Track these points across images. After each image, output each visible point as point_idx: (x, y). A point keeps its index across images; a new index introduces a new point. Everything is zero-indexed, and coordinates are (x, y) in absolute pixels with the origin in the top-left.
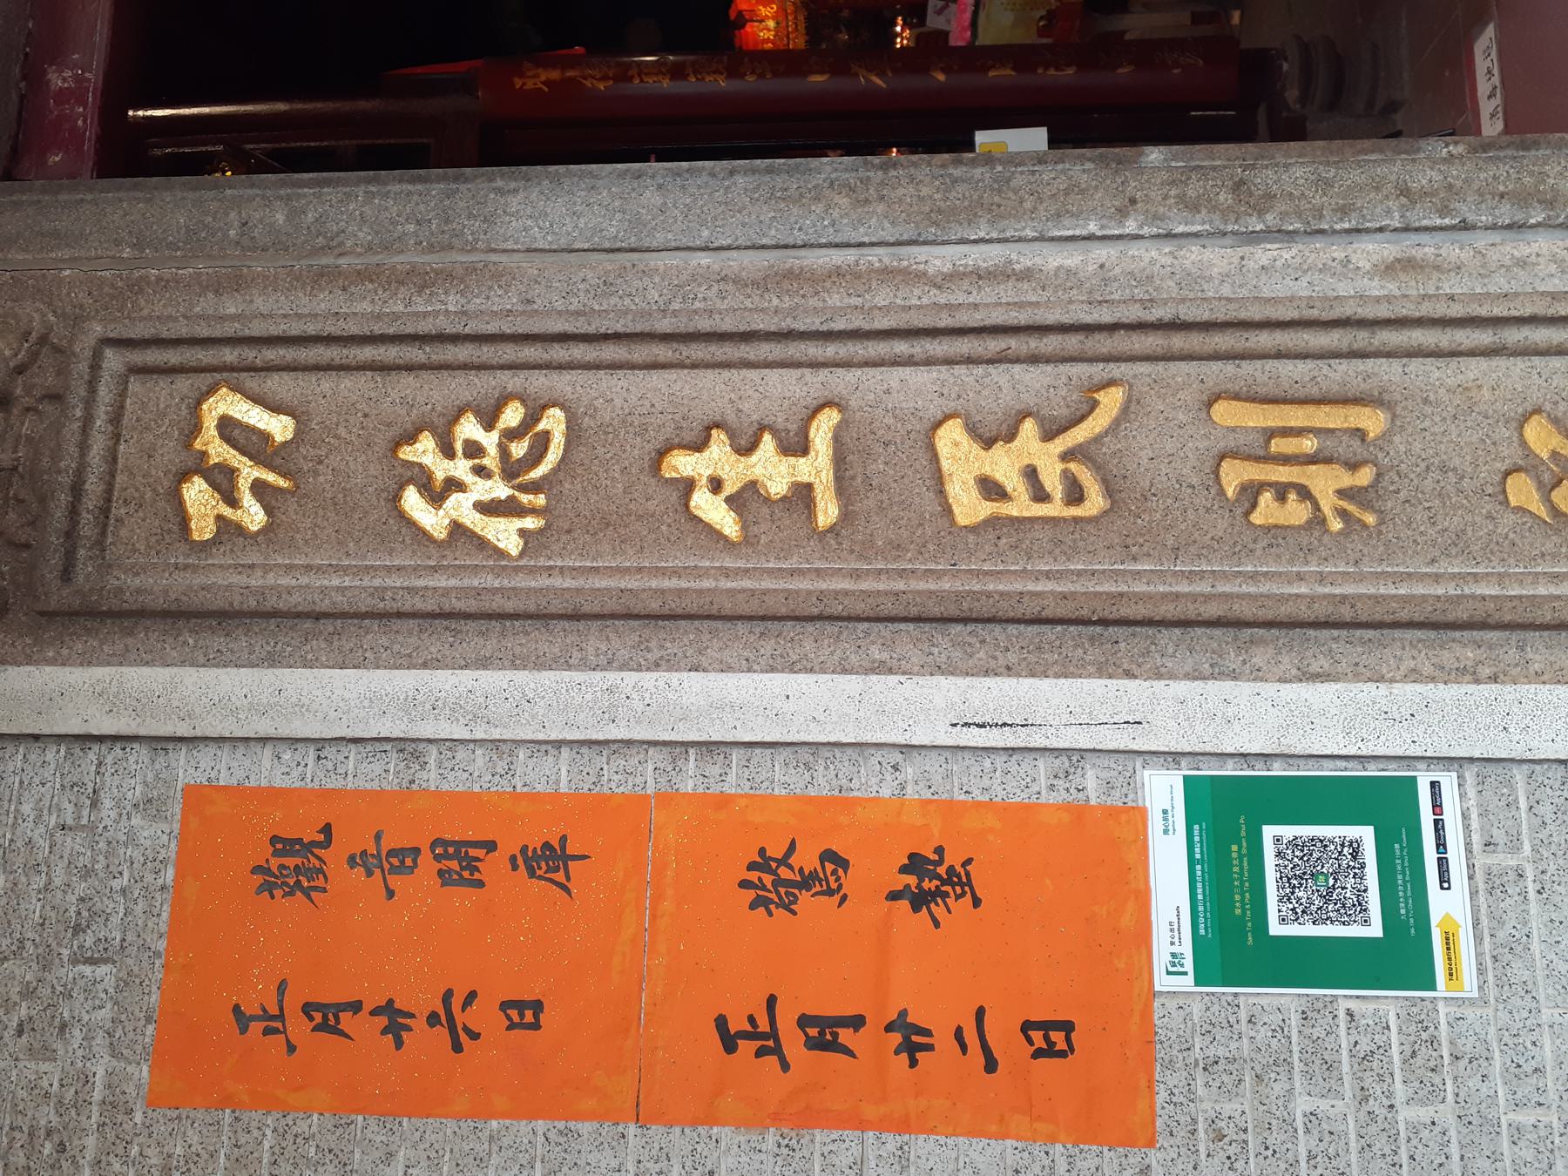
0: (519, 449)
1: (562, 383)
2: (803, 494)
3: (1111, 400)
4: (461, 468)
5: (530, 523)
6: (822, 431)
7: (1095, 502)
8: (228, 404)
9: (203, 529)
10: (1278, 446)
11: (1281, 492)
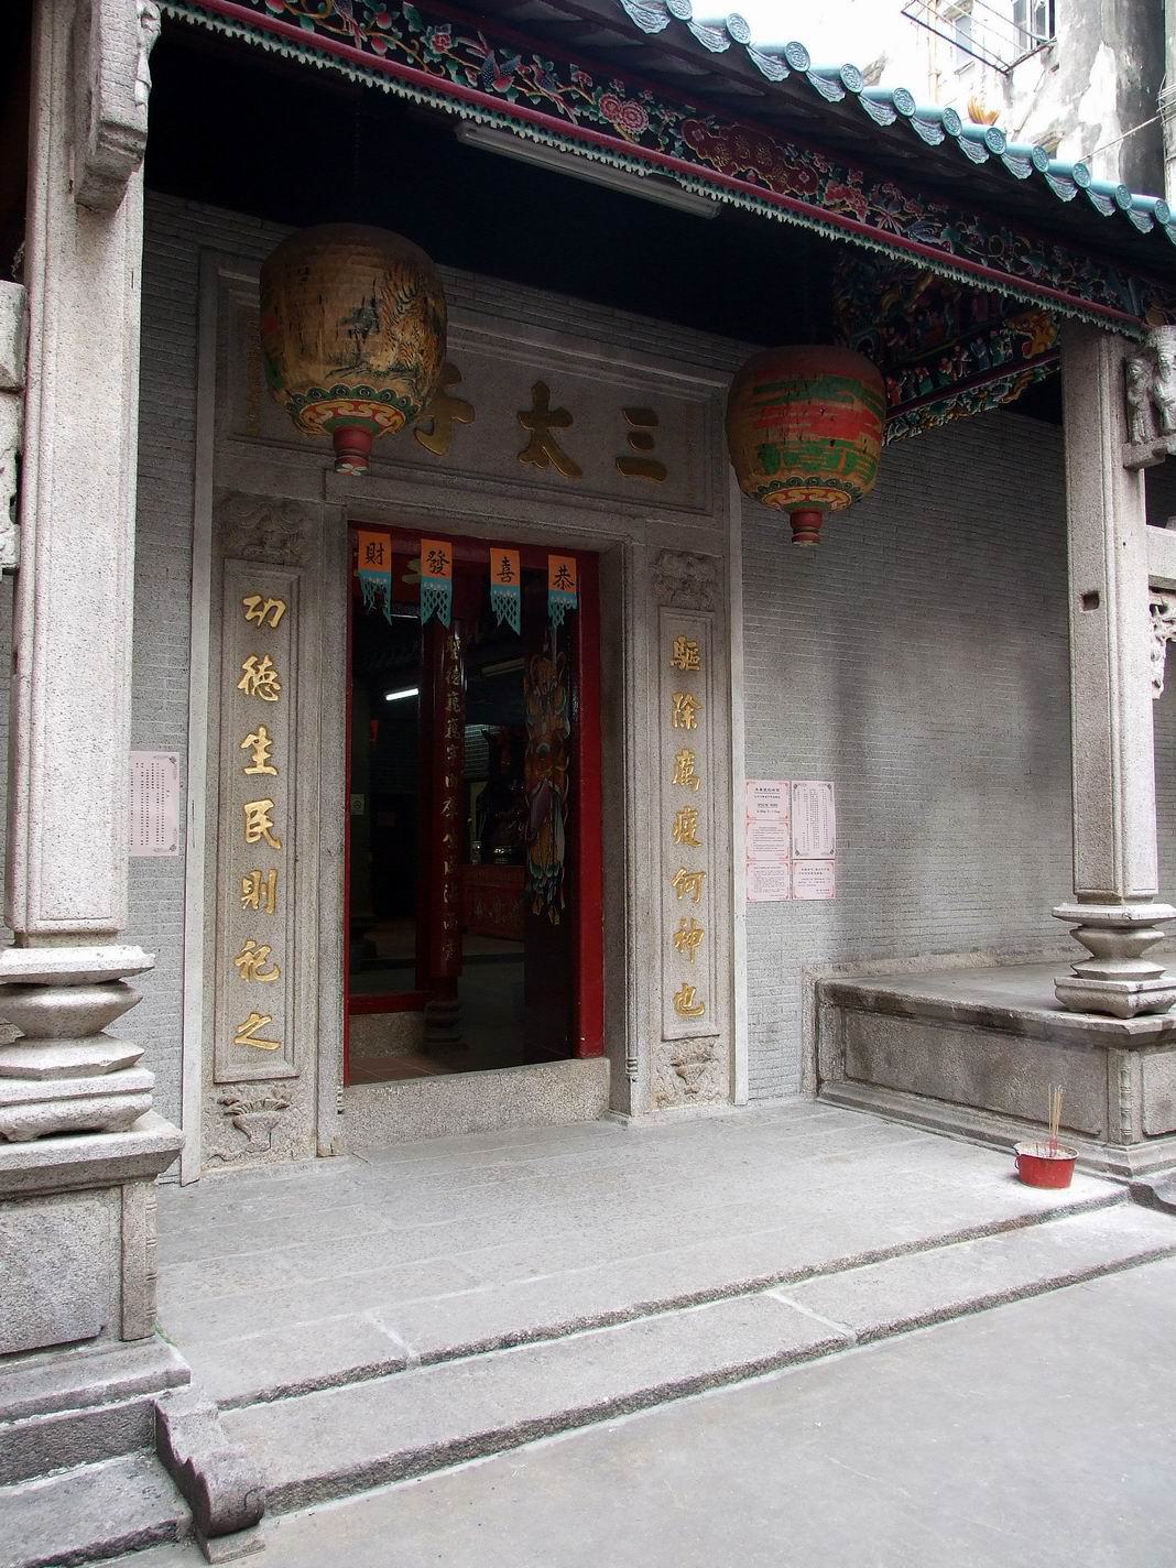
0: (267, 689)
5: (247, 690)
6: (268, 770)
8: (281, 607)
9: (246, 602)
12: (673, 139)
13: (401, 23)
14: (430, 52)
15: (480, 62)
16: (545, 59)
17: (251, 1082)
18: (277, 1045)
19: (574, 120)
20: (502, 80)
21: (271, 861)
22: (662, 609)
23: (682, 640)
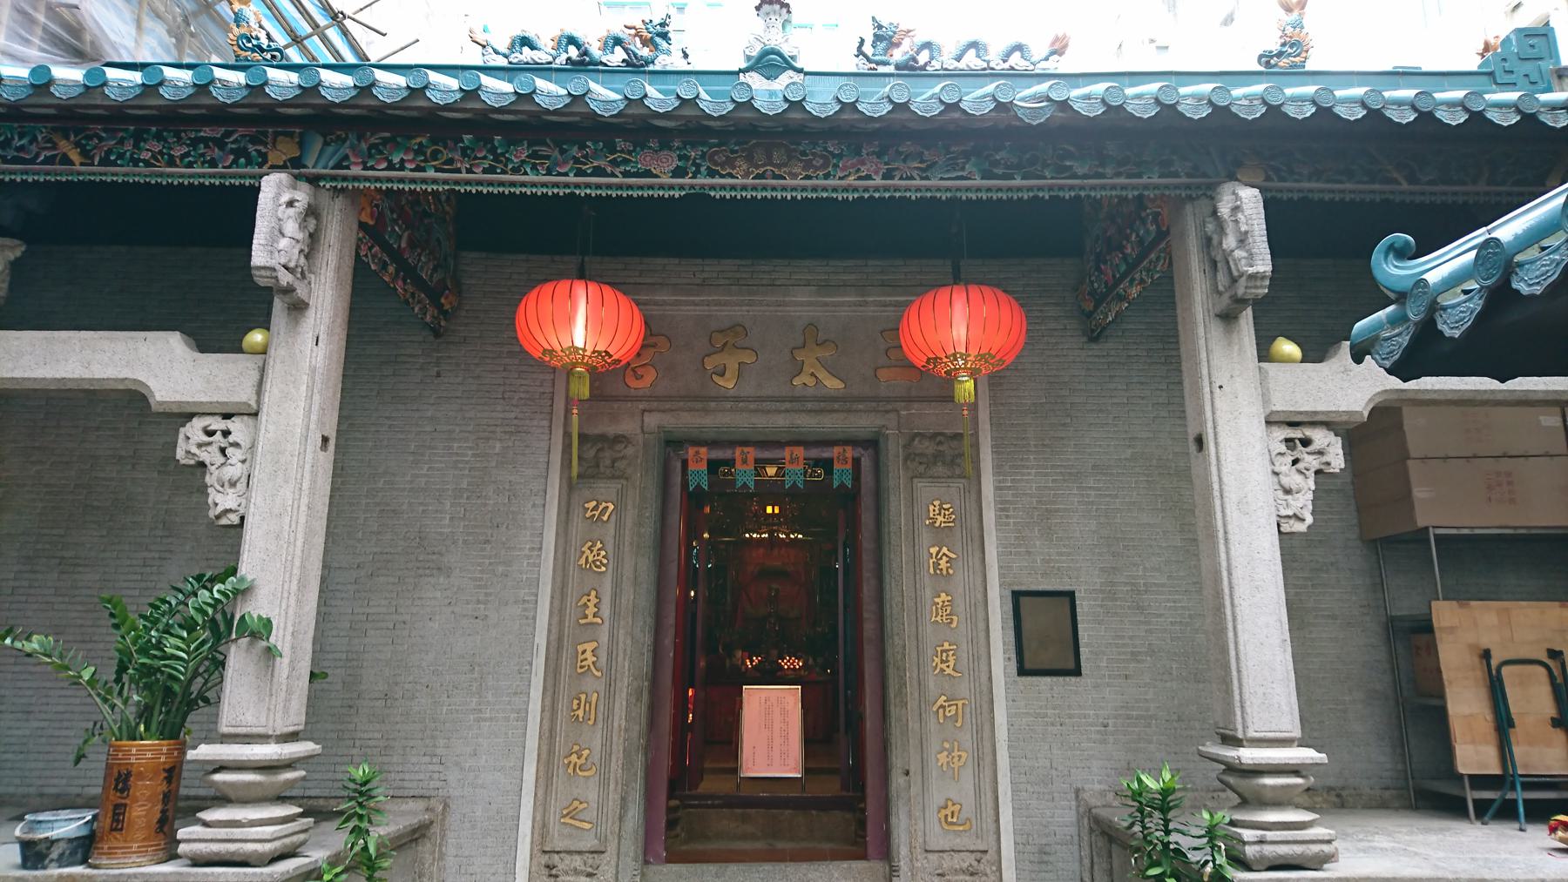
0: (598, 563)
1: (610, 571)
2: (586, 617)
3: (599, 674)
4: (595, 552)
7: (579, 671)
8: (611, 507)
9: (586, 505)
10: (588, 705)
11: (579, 704)
12: (698, 166)
13: (493, 150)
14: (512, 161)
15: (547, 157)
16: (595, 142)
17: (569, 852)
18: (590, 826)
19: (620, 175)
20: (565, 163)
21: (593, 687)
22: (915, 480)
23: (937, 503)
